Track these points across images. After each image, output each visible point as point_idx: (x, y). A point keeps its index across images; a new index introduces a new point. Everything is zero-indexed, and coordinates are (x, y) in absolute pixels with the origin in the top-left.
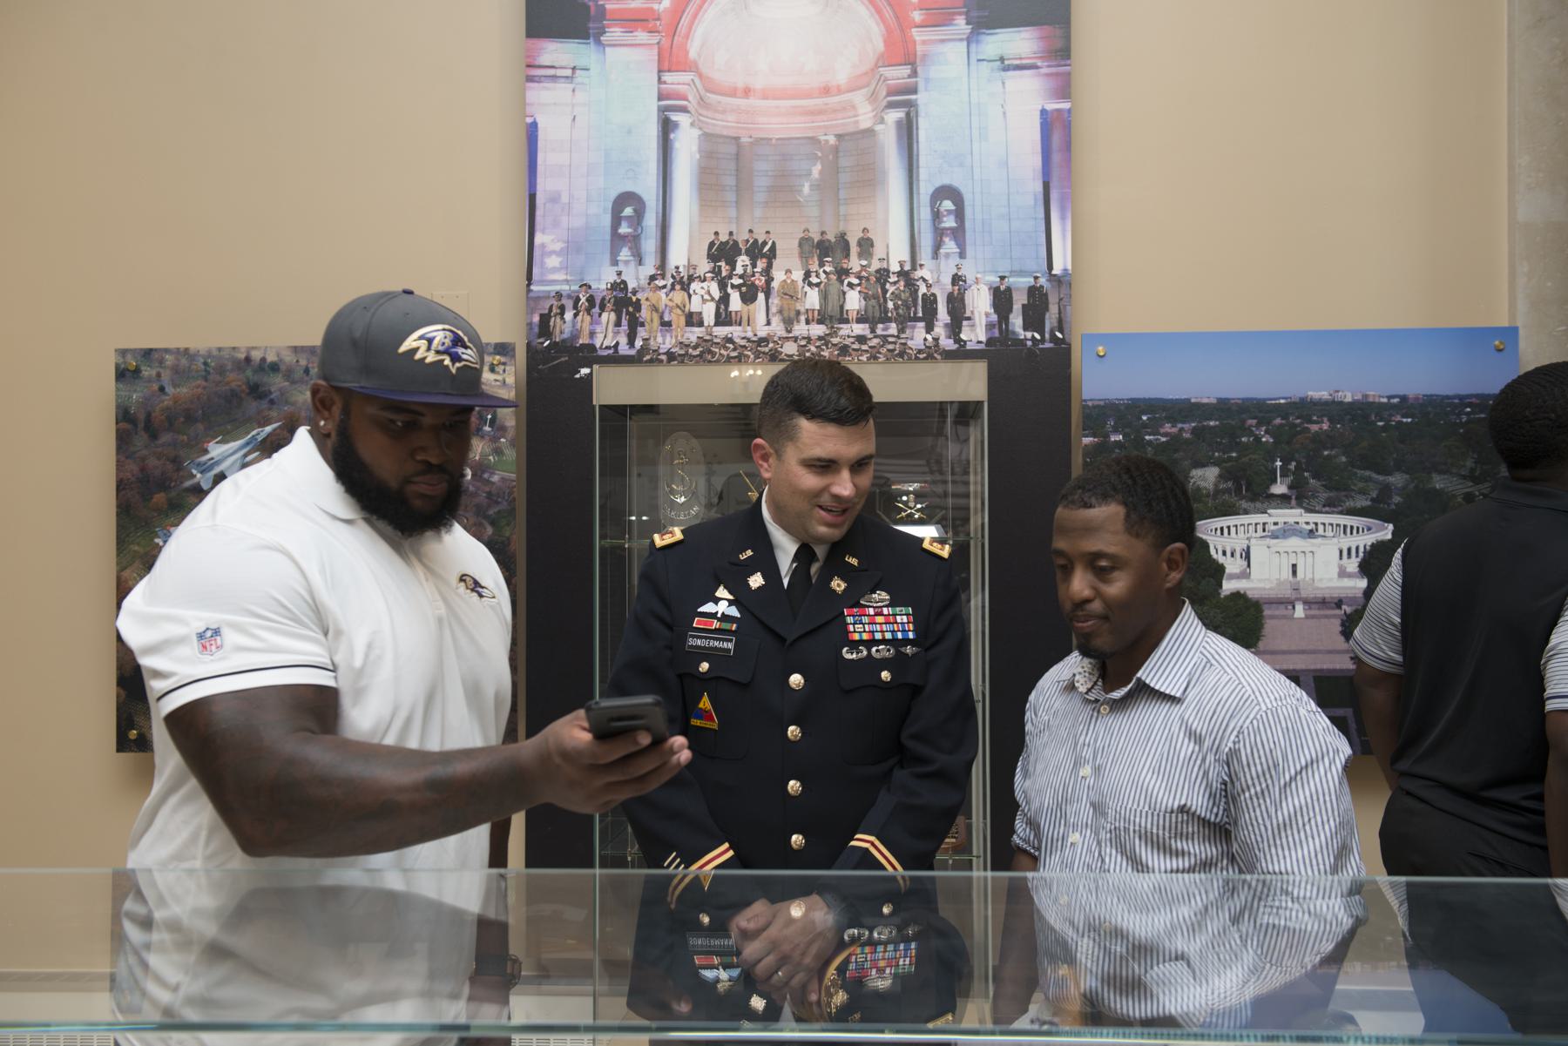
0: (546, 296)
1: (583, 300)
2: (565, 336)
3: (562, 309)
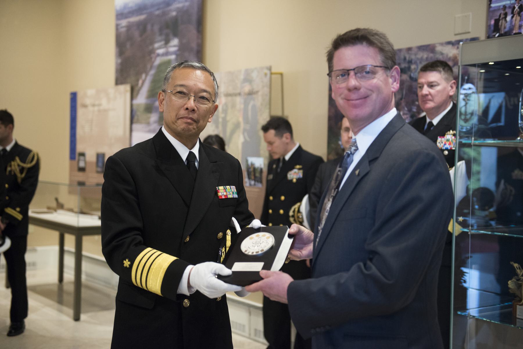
0: (498, 9)
1: (517, 7)
2: (506, 30)
3: (506, 15)
